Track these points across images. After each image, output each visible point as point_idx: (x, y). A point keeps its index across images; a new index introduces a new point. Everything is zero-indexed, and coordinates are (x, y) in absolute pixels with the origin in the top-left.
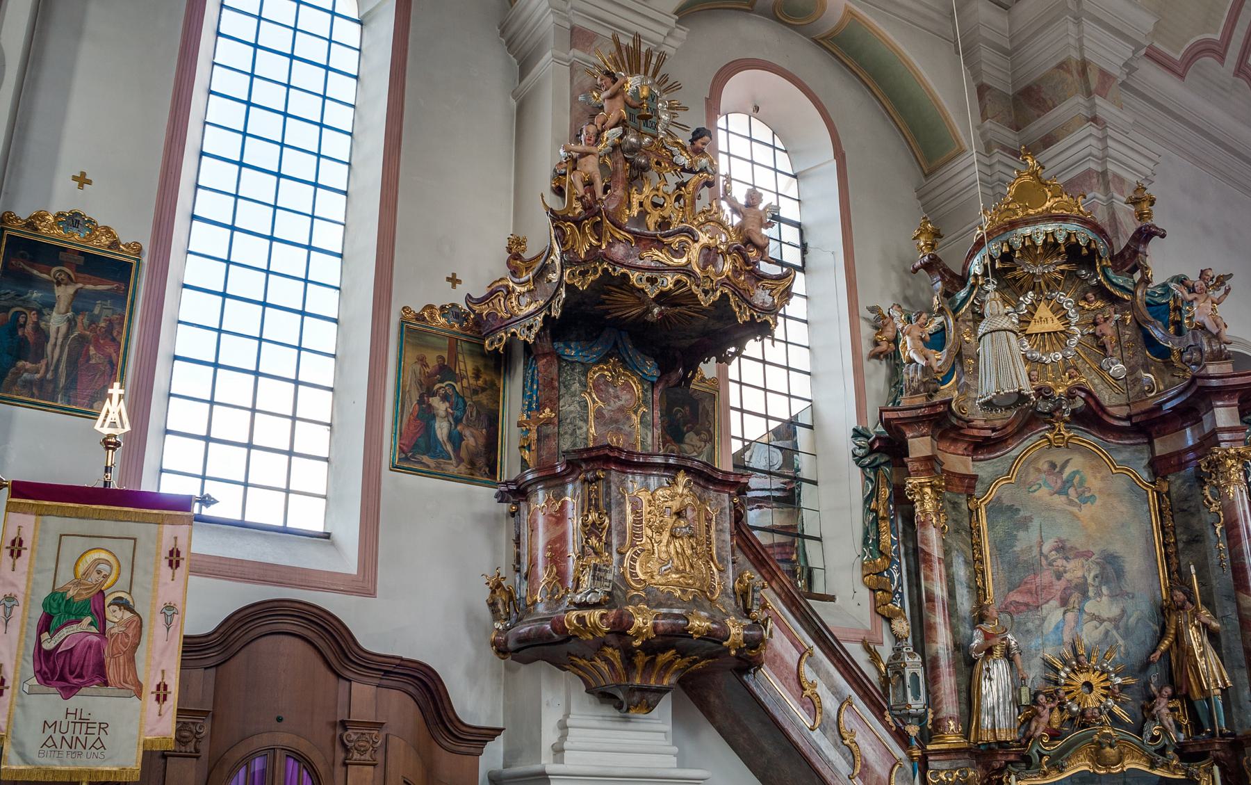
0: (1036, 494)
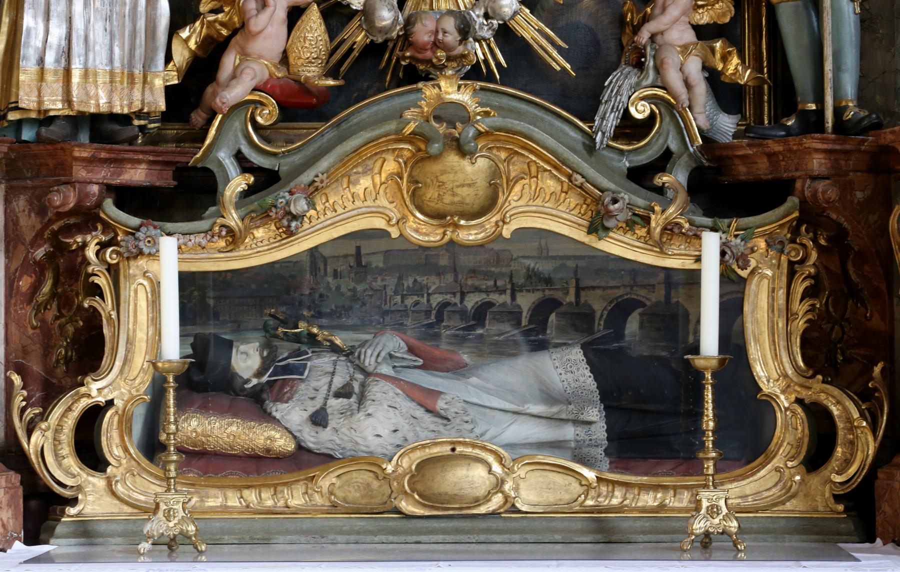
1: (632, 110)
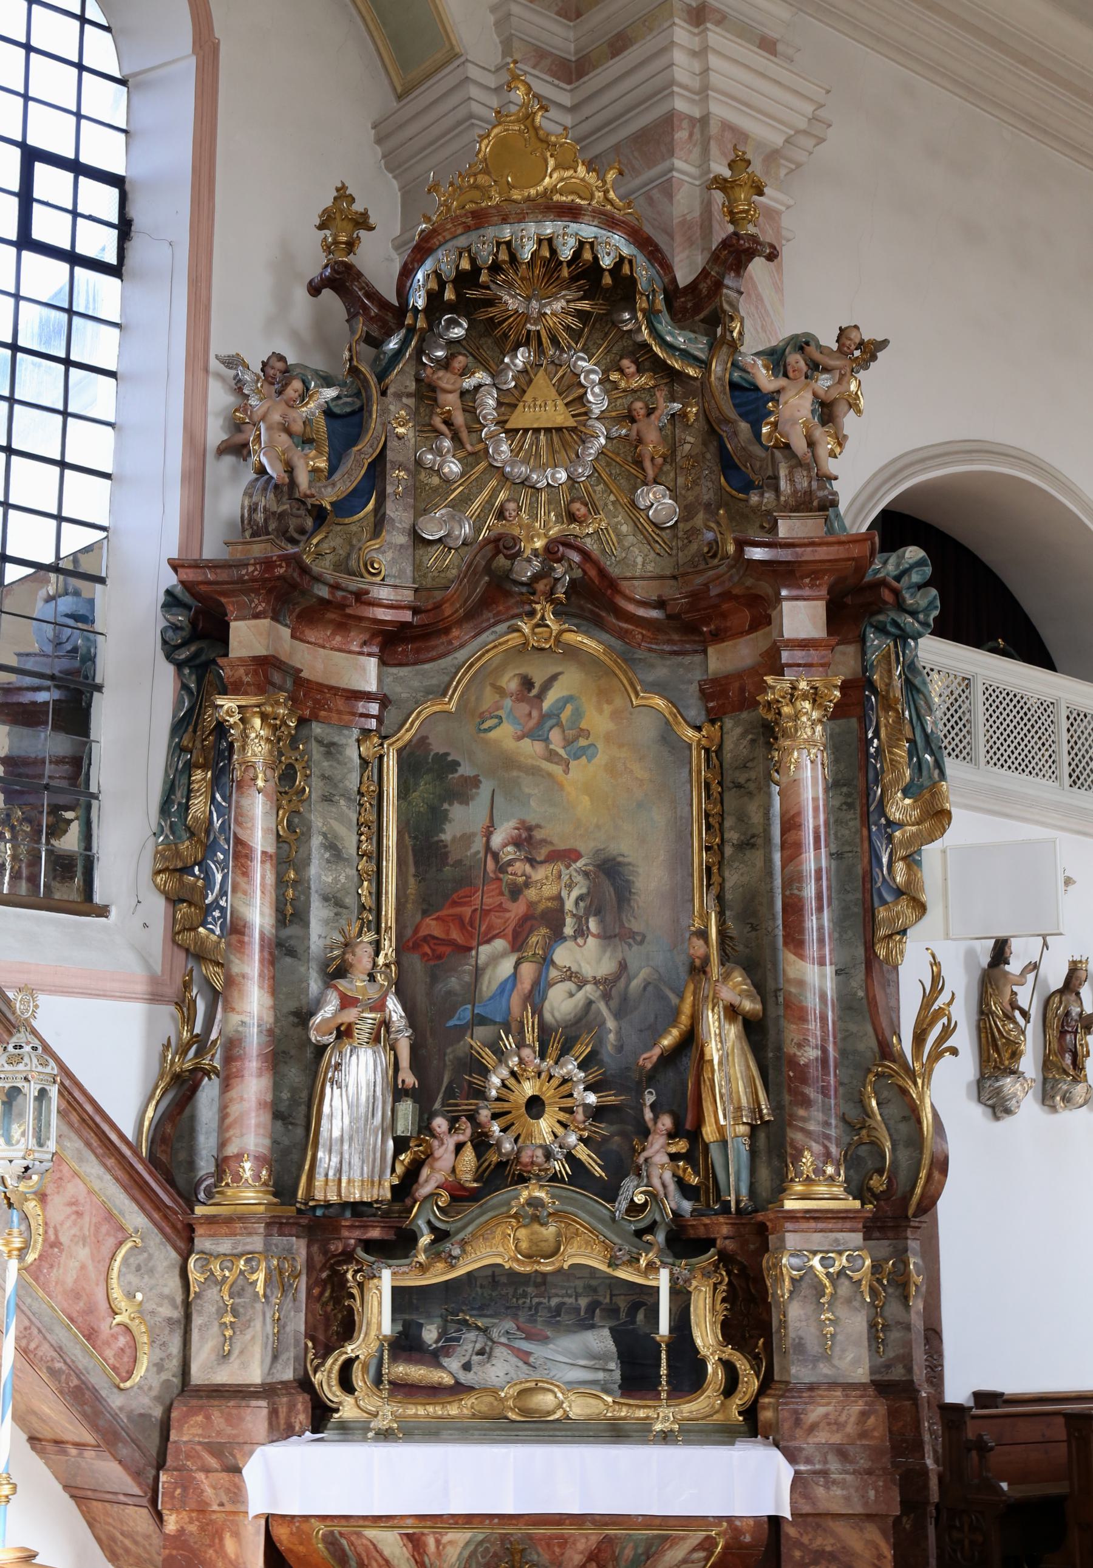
0: (492, 735)
1: (636, 1199)
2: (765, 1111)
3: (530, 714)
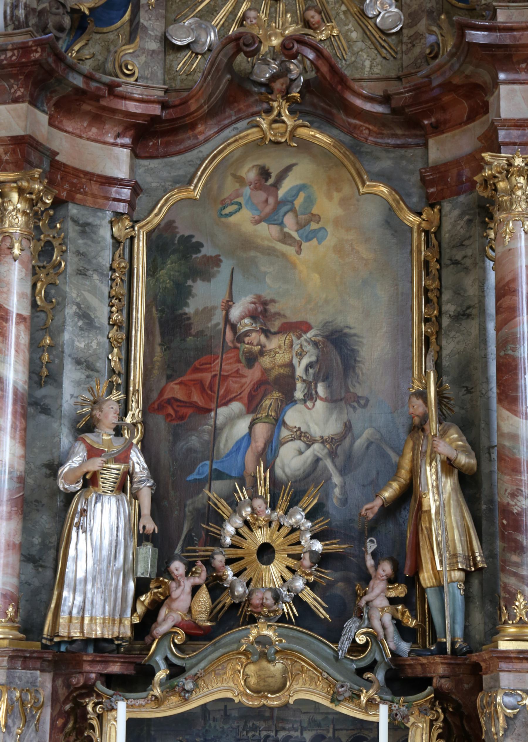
0: (232, 219)
2: (479, 559)
3: (266, 201)
